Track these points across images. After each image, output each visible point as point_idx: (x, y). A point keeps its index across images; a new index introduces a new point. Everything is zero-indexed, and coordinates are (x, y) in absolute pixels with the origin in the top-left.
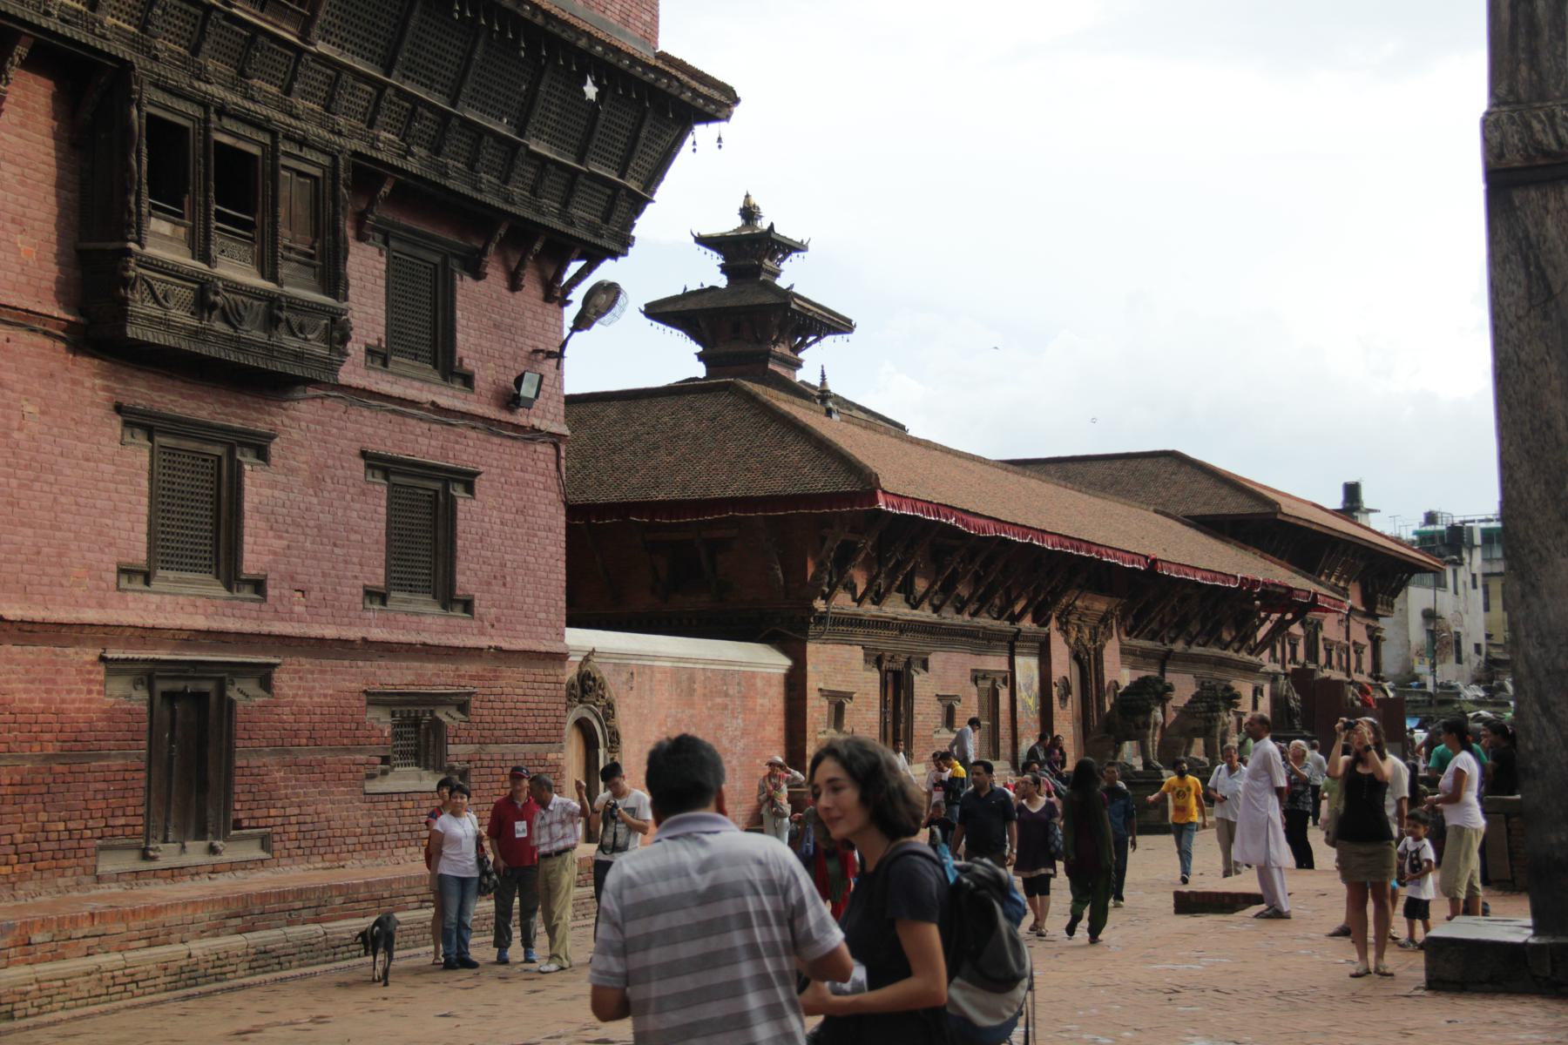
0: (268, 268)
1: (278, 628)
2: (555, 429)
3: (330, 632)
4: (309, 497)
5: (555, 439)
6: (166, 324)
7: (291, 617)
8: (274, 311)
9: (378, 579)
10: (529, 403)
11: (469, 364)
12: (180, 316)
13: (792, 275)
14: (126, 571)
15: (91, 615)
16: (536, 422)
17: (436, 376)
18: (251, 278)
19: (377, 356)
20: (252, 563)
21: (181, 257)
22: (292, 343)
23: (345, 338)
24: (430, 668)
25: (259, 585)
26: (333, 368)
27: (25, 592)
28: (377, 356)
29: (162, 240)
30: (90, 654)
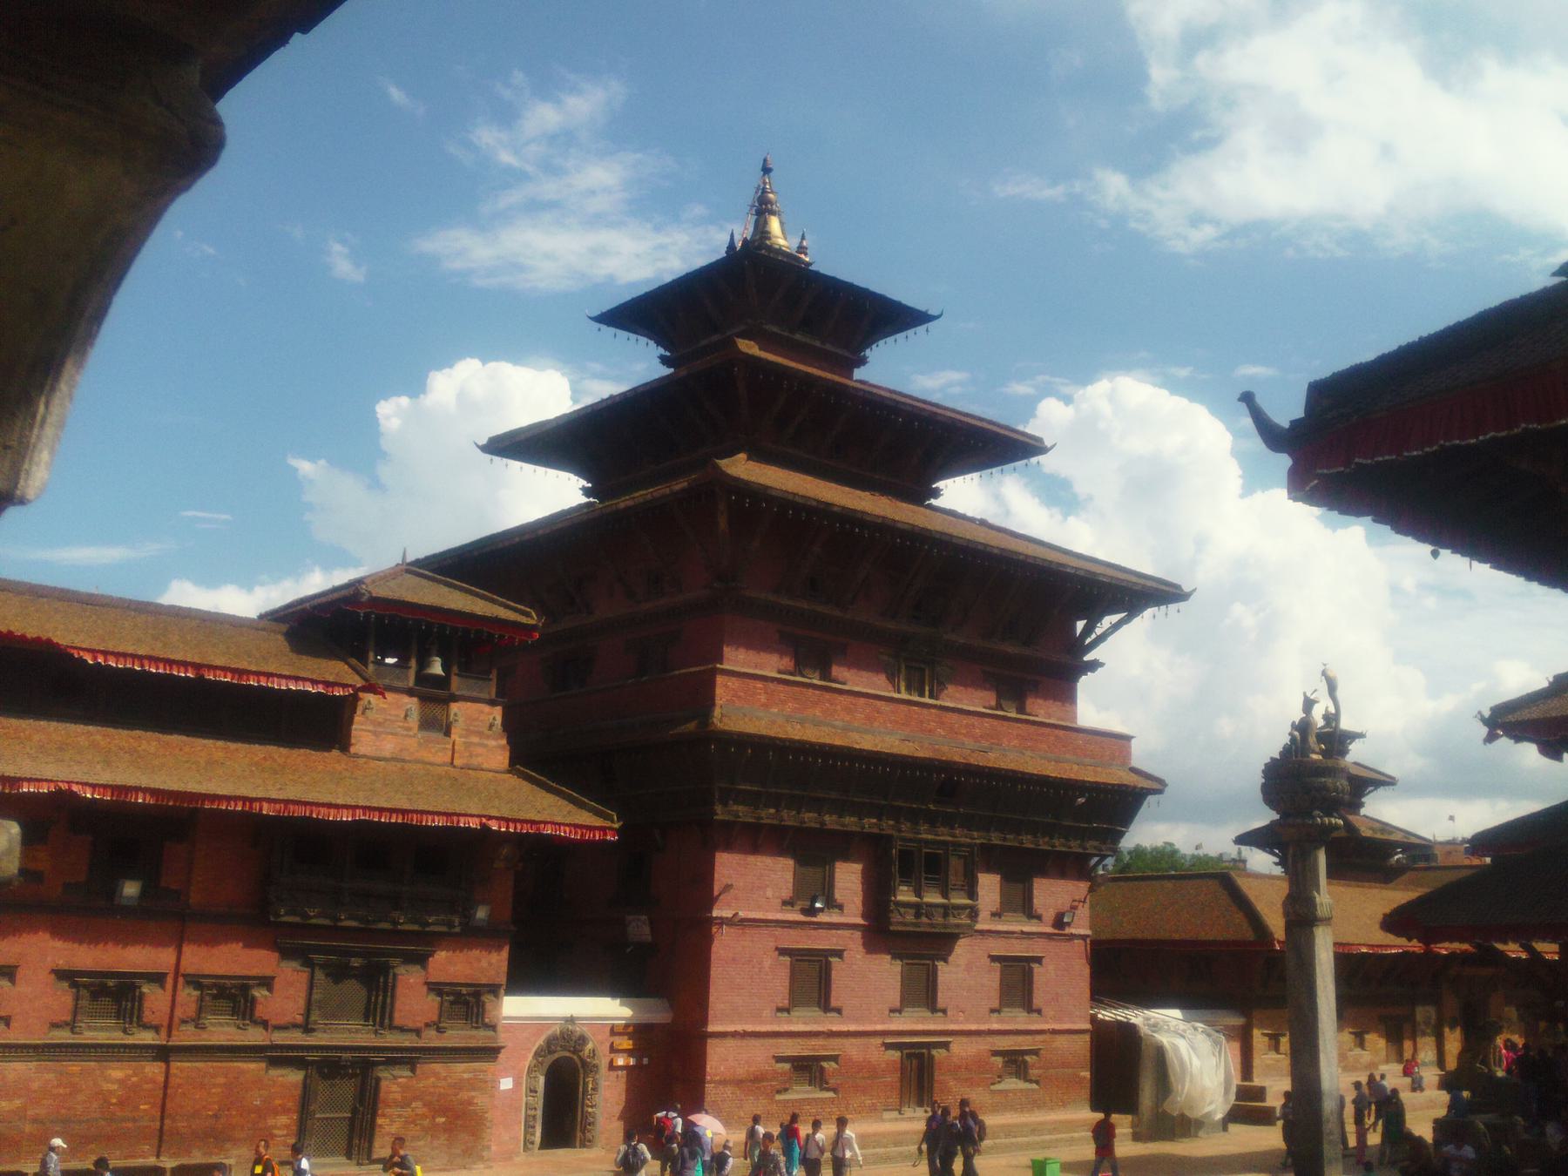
0: (945, 895)
1: (952, 1027)
2: (1083, 932)
3: (973, 1027)
4: (966, 974)
5: (1084, 937)
6: (905, 924)
7: (957, 1022)
8: (947, 910)
9: (996, 1004)
10: (1069, 924)
11: (1040, 911)
12: (910, 918)
13: (1356, 753)
14: (892, 1011)
15: (879, 1027)
16: (1073, 931)
17: (1025, 919)
18: (939, 900)
19: (996, 915)
20: (941, 1002)
21: (913, 899)
22: (953, 921)
23: (977, 915)
24: (1020, 1038)
25: (944, 1011)
26: (970, 927)
27: (856, 1020)
28: (996, 915)
29: (904, 895)
30: (879, 1041)
